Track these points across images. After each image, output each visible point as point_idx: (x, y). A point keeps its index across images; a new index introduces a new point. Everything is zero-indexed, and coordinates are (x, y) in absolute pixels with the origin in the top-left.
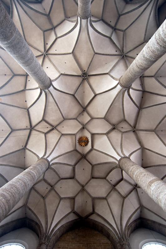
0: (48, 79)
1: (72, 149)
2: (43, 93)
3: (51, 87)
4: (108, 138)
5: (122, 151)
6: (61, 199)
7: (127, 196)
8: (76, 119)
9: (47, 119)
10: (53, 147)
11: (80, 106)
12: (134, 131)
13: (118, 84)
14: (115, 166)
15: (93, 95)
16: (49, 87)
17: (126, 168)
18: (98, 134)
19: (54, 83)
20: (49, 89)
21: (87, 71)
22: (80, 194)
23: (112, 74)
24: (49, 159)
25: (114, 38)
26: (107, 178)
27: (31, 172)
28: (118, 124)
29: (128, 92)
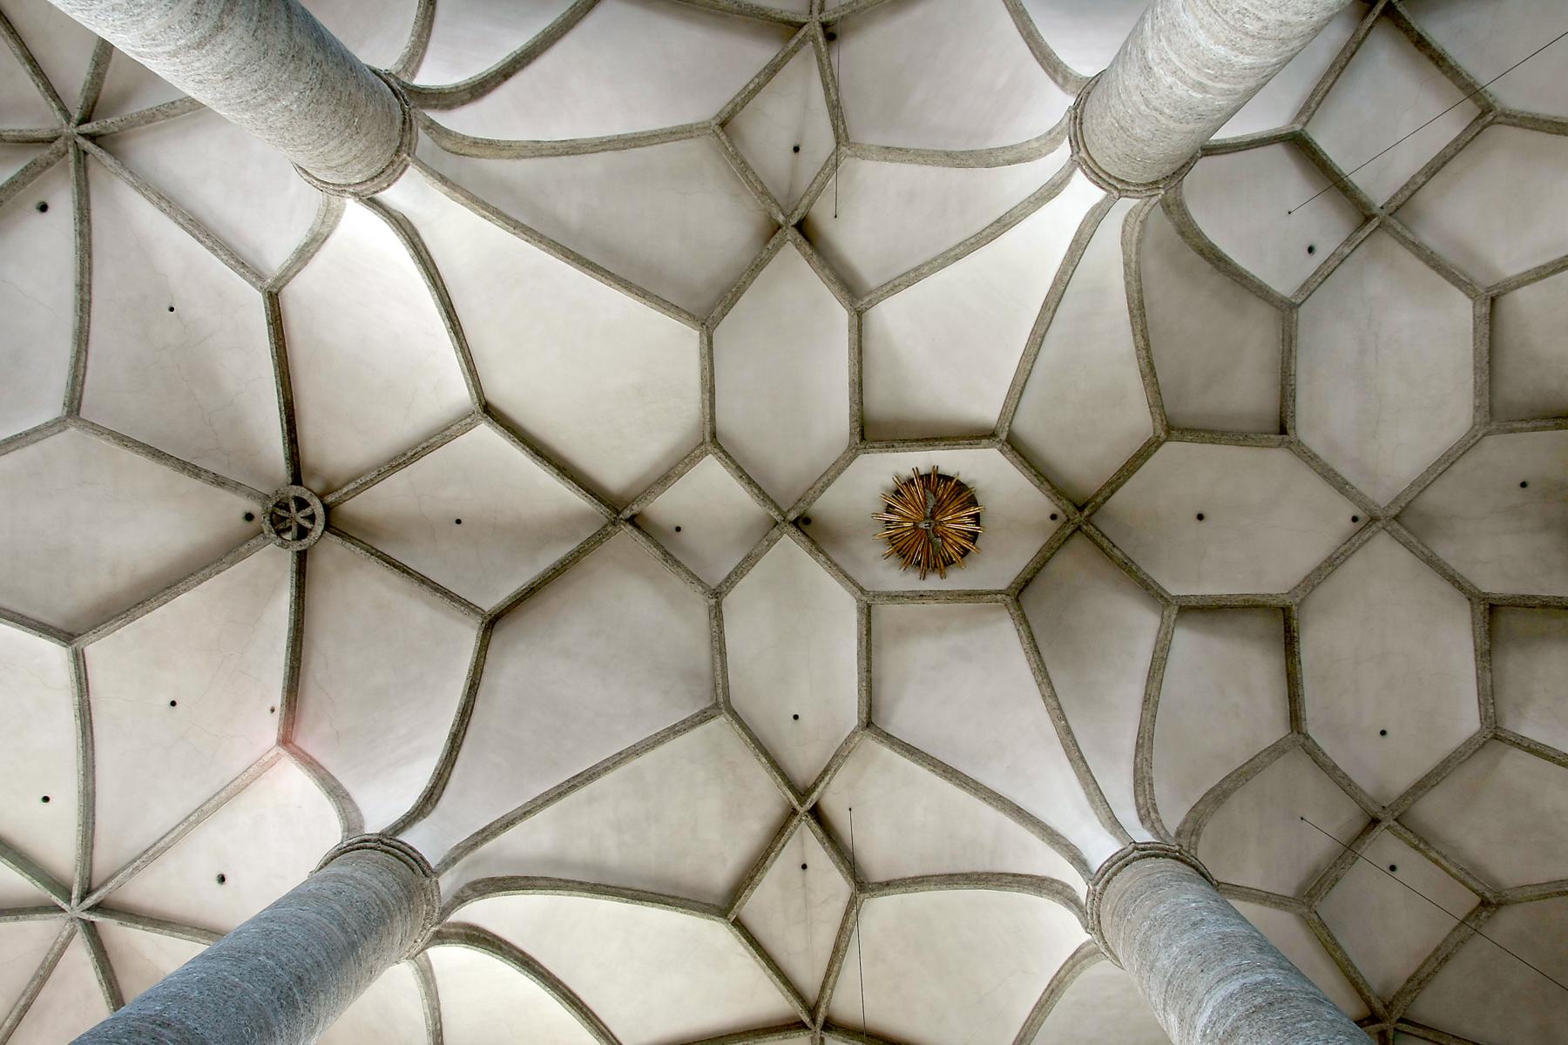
0: (338, 878)
1: (1004, 634)
2: (477, 912)
3: (410, 838)
4: (894, 286)
5: (1020, 155)
6: (1495, 735)
7: (1471, 90)
8: (716, 595)
9: (721, 875)
10: (989, 813)
11: (588, 561)
12: (831, 37)
13: (373, 203)
14: (1163, 225)
16: (412, 859)
17: (1168, 131)
18: (859, 386)
19: (377, 821)
20: (433, 859)
21: (252, 494)
22: (1446, 551)
23: (275, 258)
24: (1101, 847)
26: (1284, 286)
27: (1212, 1023)
28: (764, 193)
29: (449, 107)
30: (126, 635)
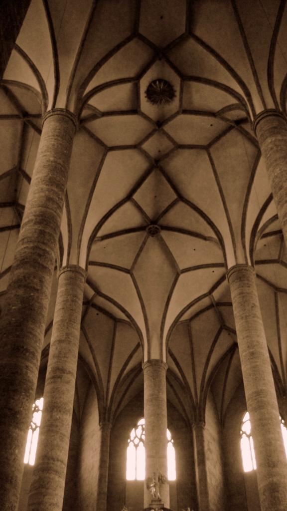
15: (136, 197)
25: (91, 293)
30: (178, 260)
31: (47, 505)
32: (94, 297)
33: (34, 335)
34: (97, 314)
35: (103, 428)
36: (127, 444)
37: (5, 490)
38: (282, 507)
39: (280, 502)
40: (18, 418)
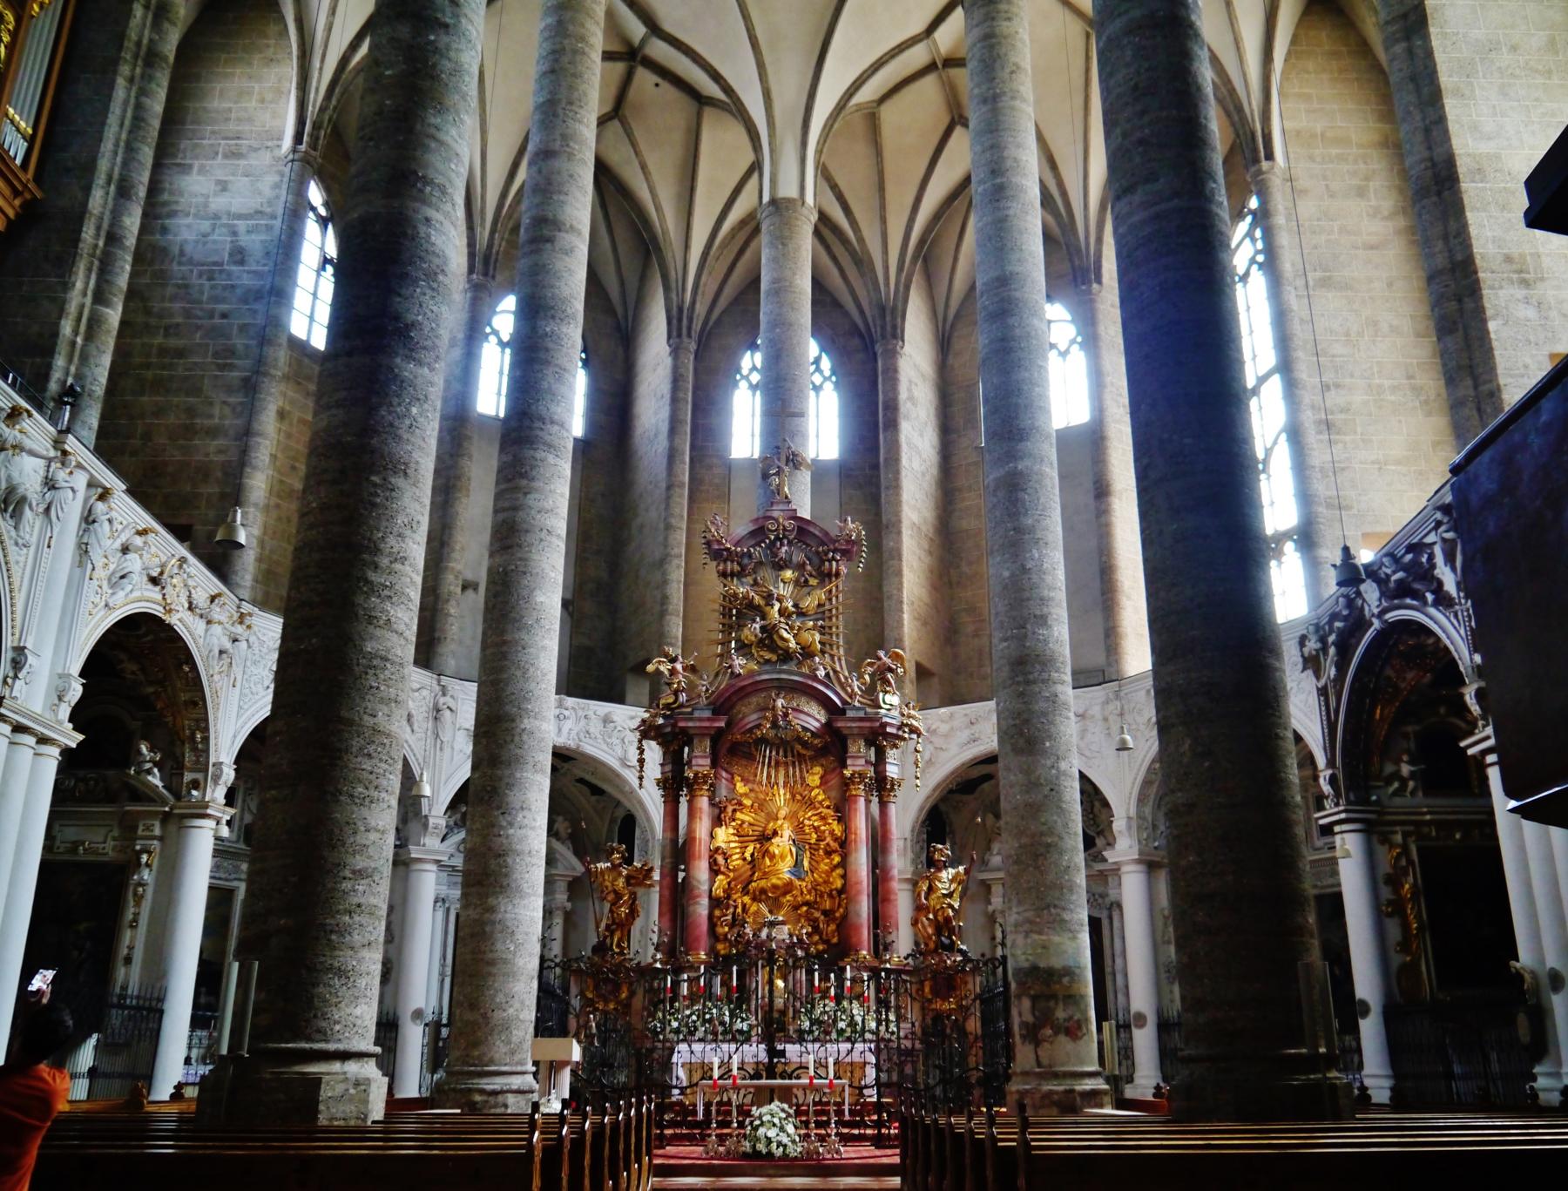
25: (637, 30)
31: (533, 512)
32: (644, 41)
33: (442, 143)
34: (657, 85)
35: (675, 352)
36: (735, 384)
37: (393, 490)
38: (1030, 521)
39: (1027, 510)
40: (412, 338)
